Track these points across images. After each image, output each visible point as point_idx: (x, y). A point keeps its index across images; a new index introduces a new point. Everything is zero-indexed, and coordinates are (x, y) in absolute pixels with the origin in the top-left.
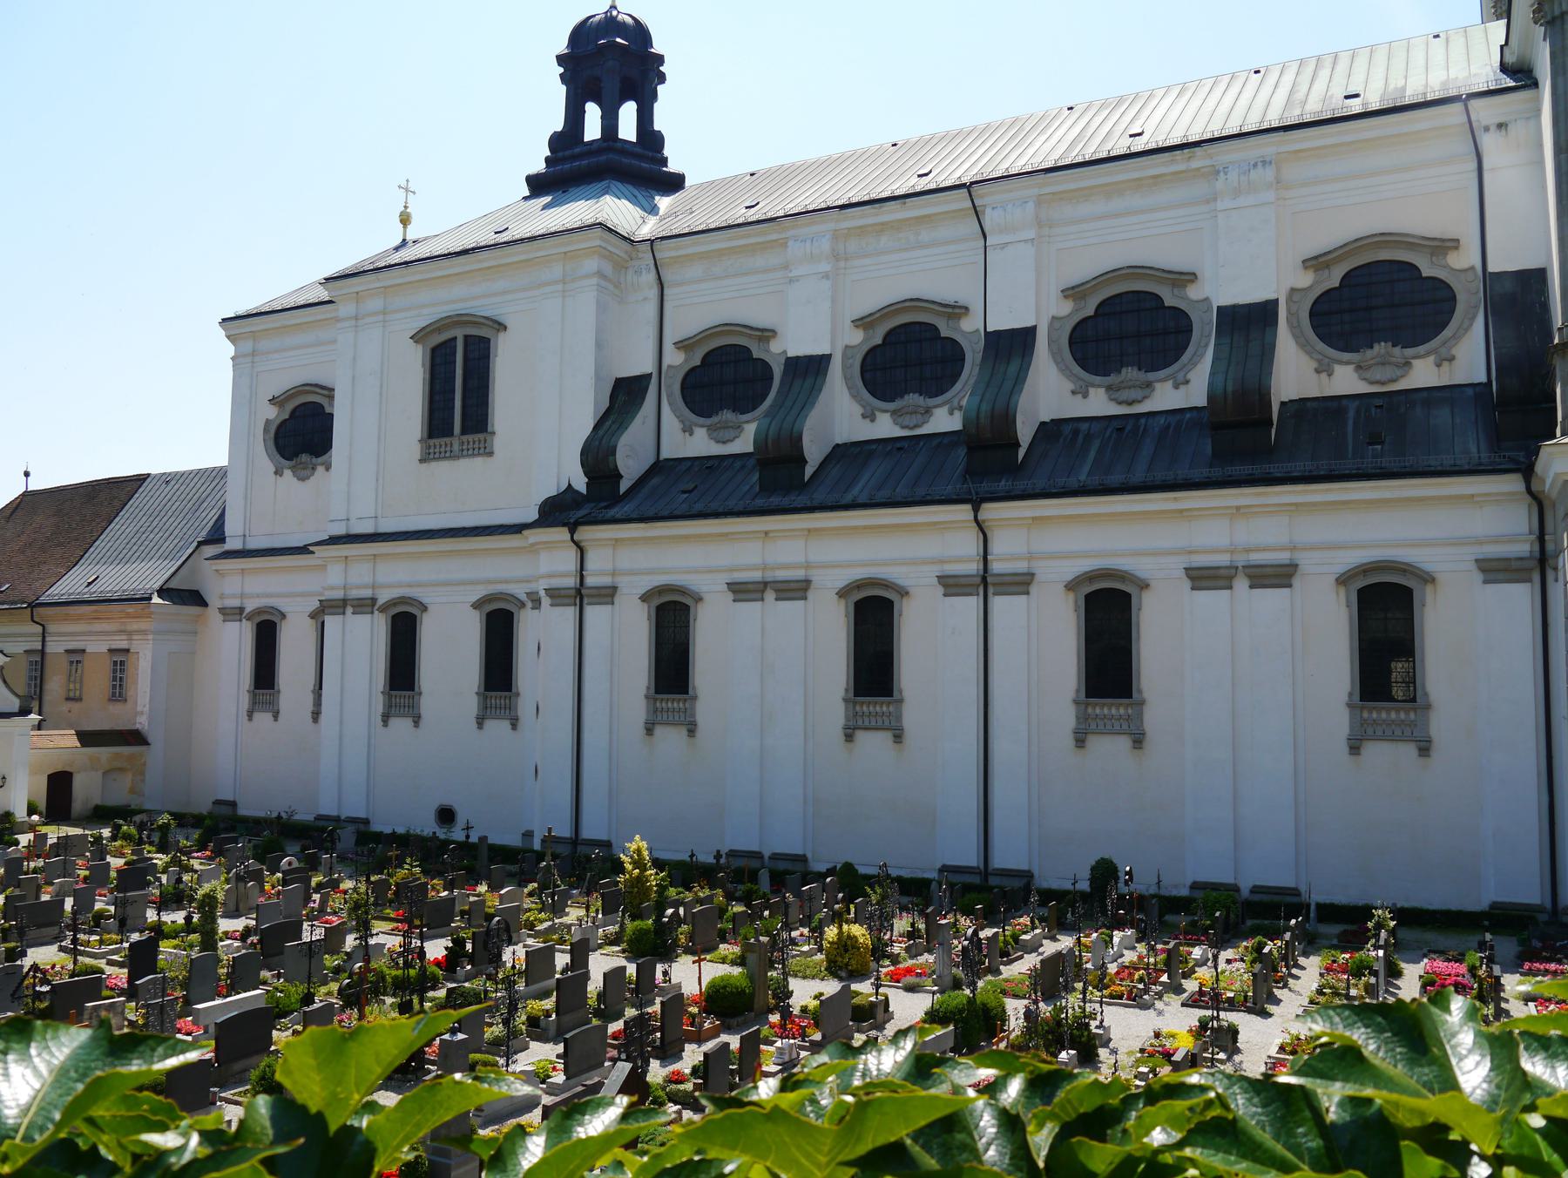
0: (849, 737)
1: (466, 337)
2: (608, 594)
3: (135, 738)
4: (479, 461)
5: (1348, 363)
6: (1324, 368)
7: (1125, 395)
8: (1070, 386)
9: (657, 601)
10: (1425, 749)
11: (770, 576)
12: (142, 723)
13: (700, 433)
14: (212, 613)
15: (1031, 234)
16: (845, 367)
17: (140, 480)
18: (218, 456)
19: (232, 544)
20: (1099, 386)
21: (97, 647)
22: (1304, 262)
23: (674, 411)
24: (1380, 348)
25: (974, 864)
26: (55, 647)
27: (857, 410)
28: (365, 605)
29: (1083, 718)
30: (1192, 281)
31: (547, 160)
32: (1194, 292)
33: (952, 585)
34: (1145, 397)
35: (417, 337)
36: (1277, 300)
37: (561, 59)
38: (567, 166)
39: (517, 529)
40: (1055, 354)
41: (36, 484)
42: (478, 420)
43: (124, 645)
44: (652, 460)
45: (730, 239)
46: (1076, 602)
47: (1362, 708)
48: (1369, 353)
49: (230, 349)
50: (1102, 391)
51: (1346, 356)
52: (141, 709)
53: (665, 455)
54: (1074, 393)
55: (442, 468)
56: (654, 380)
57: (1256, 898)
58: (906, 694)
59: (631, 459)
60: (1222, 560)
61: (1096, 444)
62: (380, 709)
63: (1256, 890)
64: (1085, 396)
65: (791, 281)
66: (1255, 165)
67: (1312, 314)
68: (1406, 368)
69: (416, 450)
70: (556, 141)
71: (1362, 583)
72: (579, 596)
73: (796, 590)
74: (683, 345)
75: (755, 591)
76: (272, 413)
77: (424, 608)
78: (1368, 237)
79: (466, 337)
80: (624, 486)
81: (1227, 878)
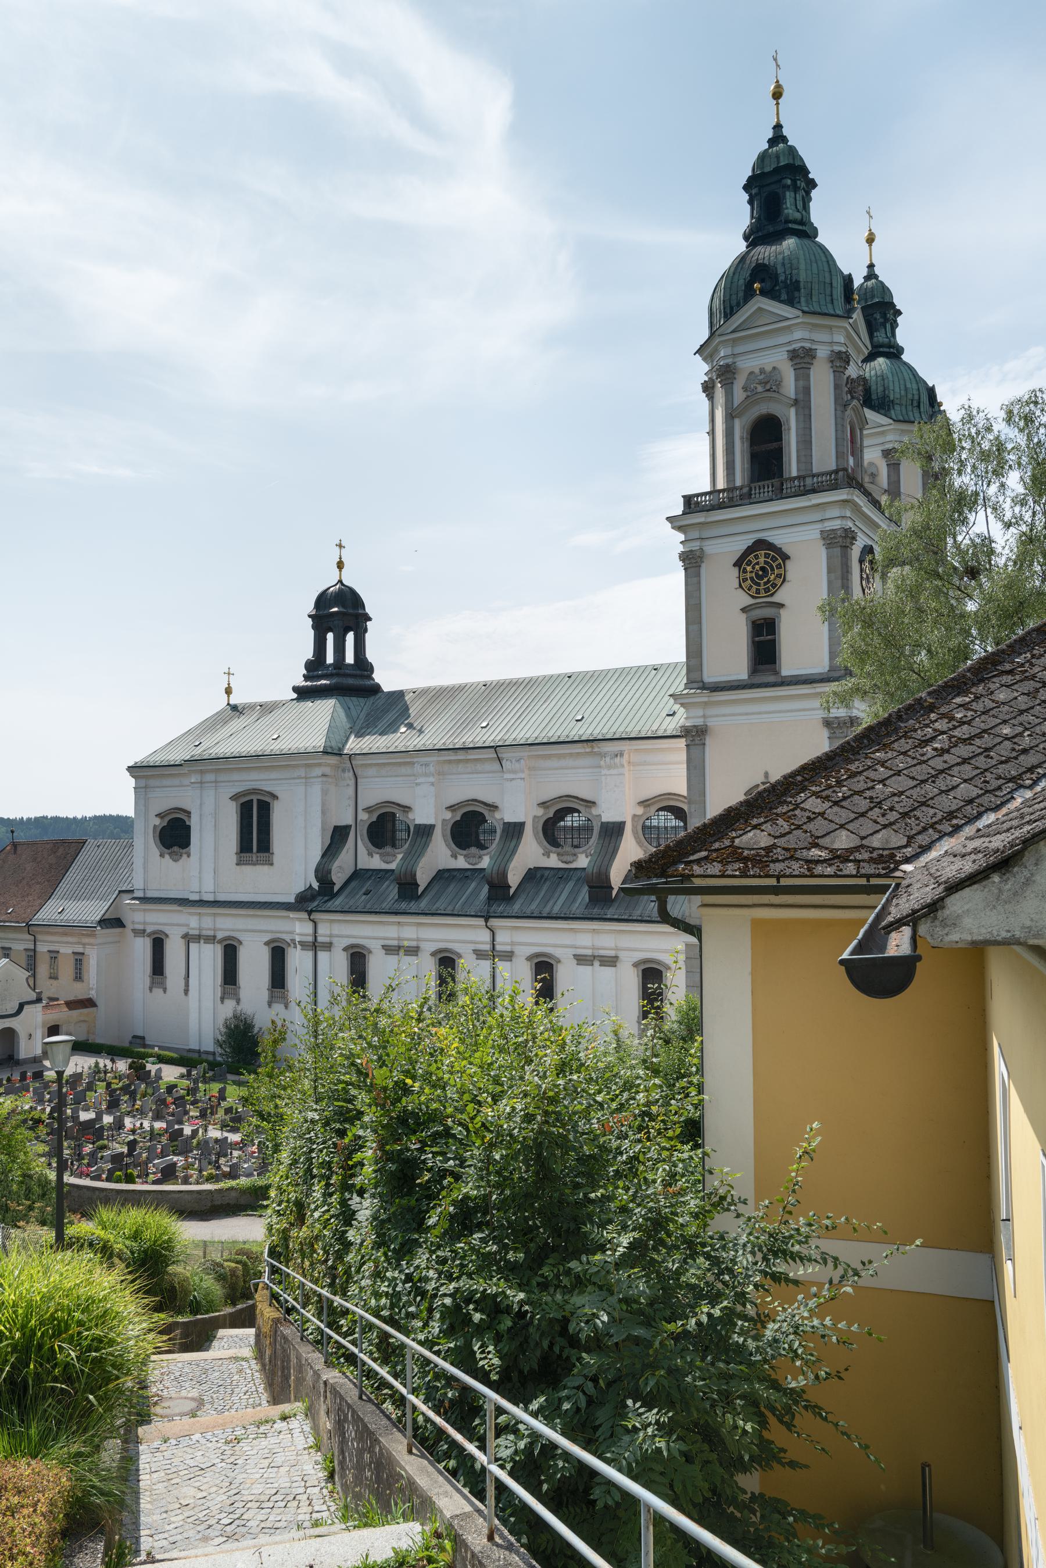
1: (258, 800)
2: (328, 946)
3: (88, 1003)
4: (266, 868)
7: (565, 858)
12: (93, 994)
13: (377, 857)
14: (128, 931)
21: (66, 950)
26: (42, 948)
28: (211, 939)
33: (480, 955)
36: (624, 823)
40: (536, 835)
42: (265, 846)
43: (81, 950)
44: (352, 870)
49: (132, 782)
52: (92, 984)
53: (359, 866)
55: (247, 869)
56: (353, 828)
59: (340, 871)
60: (589, 952)
62: (219, 995)
64: (549, 857)
65: (417, 784)
69: (234, 858)
70: (310, 666)
72: (314, 946)
74: (368, 810)
76: (157, 821)
79: (258, 800)
80: (336, 888)
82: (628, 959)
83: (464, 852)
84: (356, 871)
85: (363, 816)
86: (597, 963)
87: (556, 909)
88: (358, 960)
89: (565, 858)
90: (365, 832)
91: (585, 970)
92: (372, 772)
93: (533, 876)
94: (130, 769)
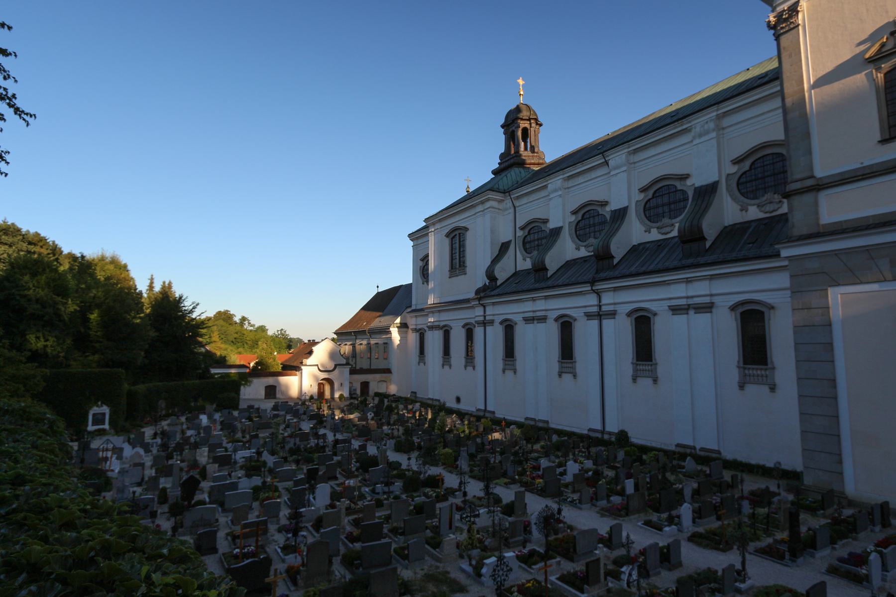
0: (560, 376)
1: (460, 234)
2: (492, 322)
4: (463, 276)
5: (754, 205)
6: (744, 209)
7: (664, 230)
8: (643, 229)
9: (505, 325)
10: (773, 388)
11: (691, 301)
15: (624, 168)
16: (570, 230)
17: (401, 286)
18: (409, 280)
19: (413, 307)
20: (654, 228)
22: (731, 161)
23: (520, 252)
24: (768, 196)
25: (600, 429)
27: (574, 246)
29: (635, 370)
30: (687, 178)
31: (499, 164)
32: (689, 182)
33: (589, 316)
34: (672, 231)
35: (447, 235)
37: (503, 126)
38: (507, 164)
39: (467, 301)
40: (638, 216)
41: (380, 290)
45: (532, 187)
46: (631, 322)
47: (745, 369)
48: (765, 198)
50: (655, 229)
51: (753, 202)
54: (646, 231)
56: (513, 243)
57: (702, 453)
58: (577, 359)
59: (503, 273)
60: (683, 302)
61: (648, 252)
63: (702, 449)
64: (650, 233)
65: (551, 199)
66: (707, 122)
67: (738, 184)
68: (780, 204)
69: (448, 274)
70: (502, 156)
71: (741, 310)
72: (485, 323)
73: (543, 319)
74: (522, 228)
75: (531, 320)
77: (451, 329)
78: (757, 146)
79: (460, 234)
80: (499, 283)
81: (690, 443)
82: (724, 304)
83: (584, 244)
84: (516, 272)
85: (520, 233)
86: (691, 312)
87: (651, 268)
88: (509, 328)
89: (664, 230)
90: (521, 244)
91: (681, 319)
92: (524, 200)
93: (636, 251)
94: (410, 236)
